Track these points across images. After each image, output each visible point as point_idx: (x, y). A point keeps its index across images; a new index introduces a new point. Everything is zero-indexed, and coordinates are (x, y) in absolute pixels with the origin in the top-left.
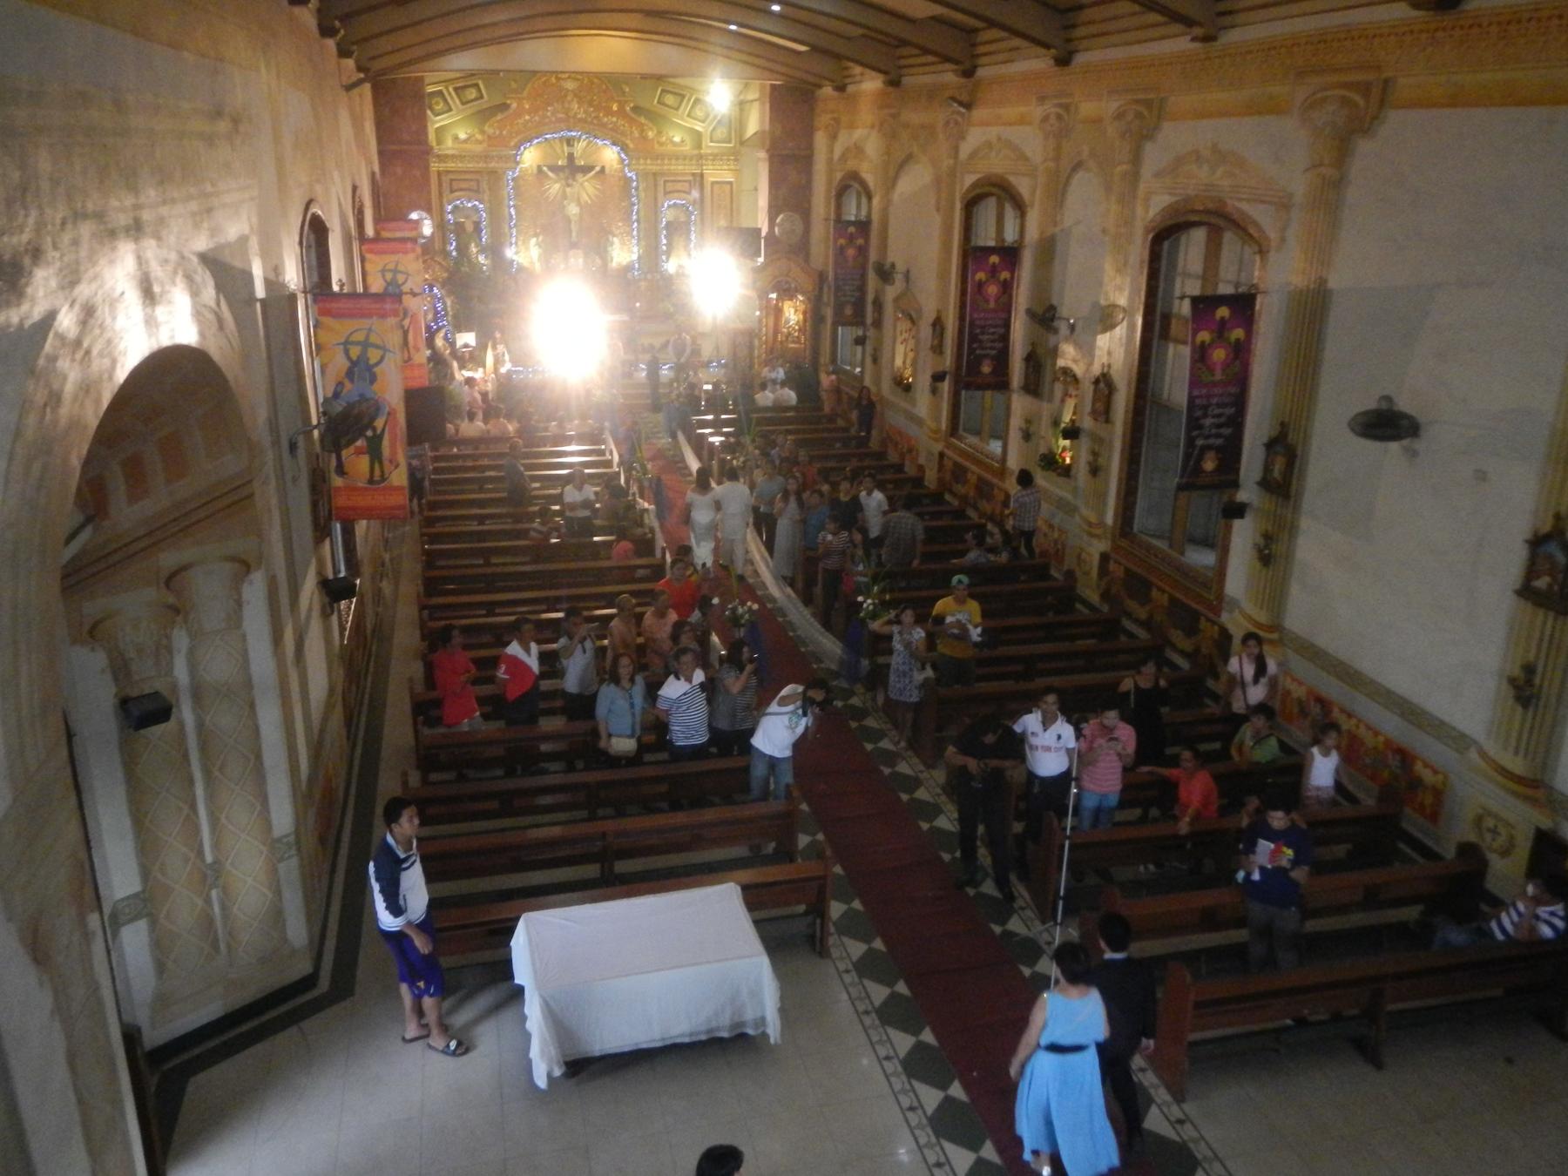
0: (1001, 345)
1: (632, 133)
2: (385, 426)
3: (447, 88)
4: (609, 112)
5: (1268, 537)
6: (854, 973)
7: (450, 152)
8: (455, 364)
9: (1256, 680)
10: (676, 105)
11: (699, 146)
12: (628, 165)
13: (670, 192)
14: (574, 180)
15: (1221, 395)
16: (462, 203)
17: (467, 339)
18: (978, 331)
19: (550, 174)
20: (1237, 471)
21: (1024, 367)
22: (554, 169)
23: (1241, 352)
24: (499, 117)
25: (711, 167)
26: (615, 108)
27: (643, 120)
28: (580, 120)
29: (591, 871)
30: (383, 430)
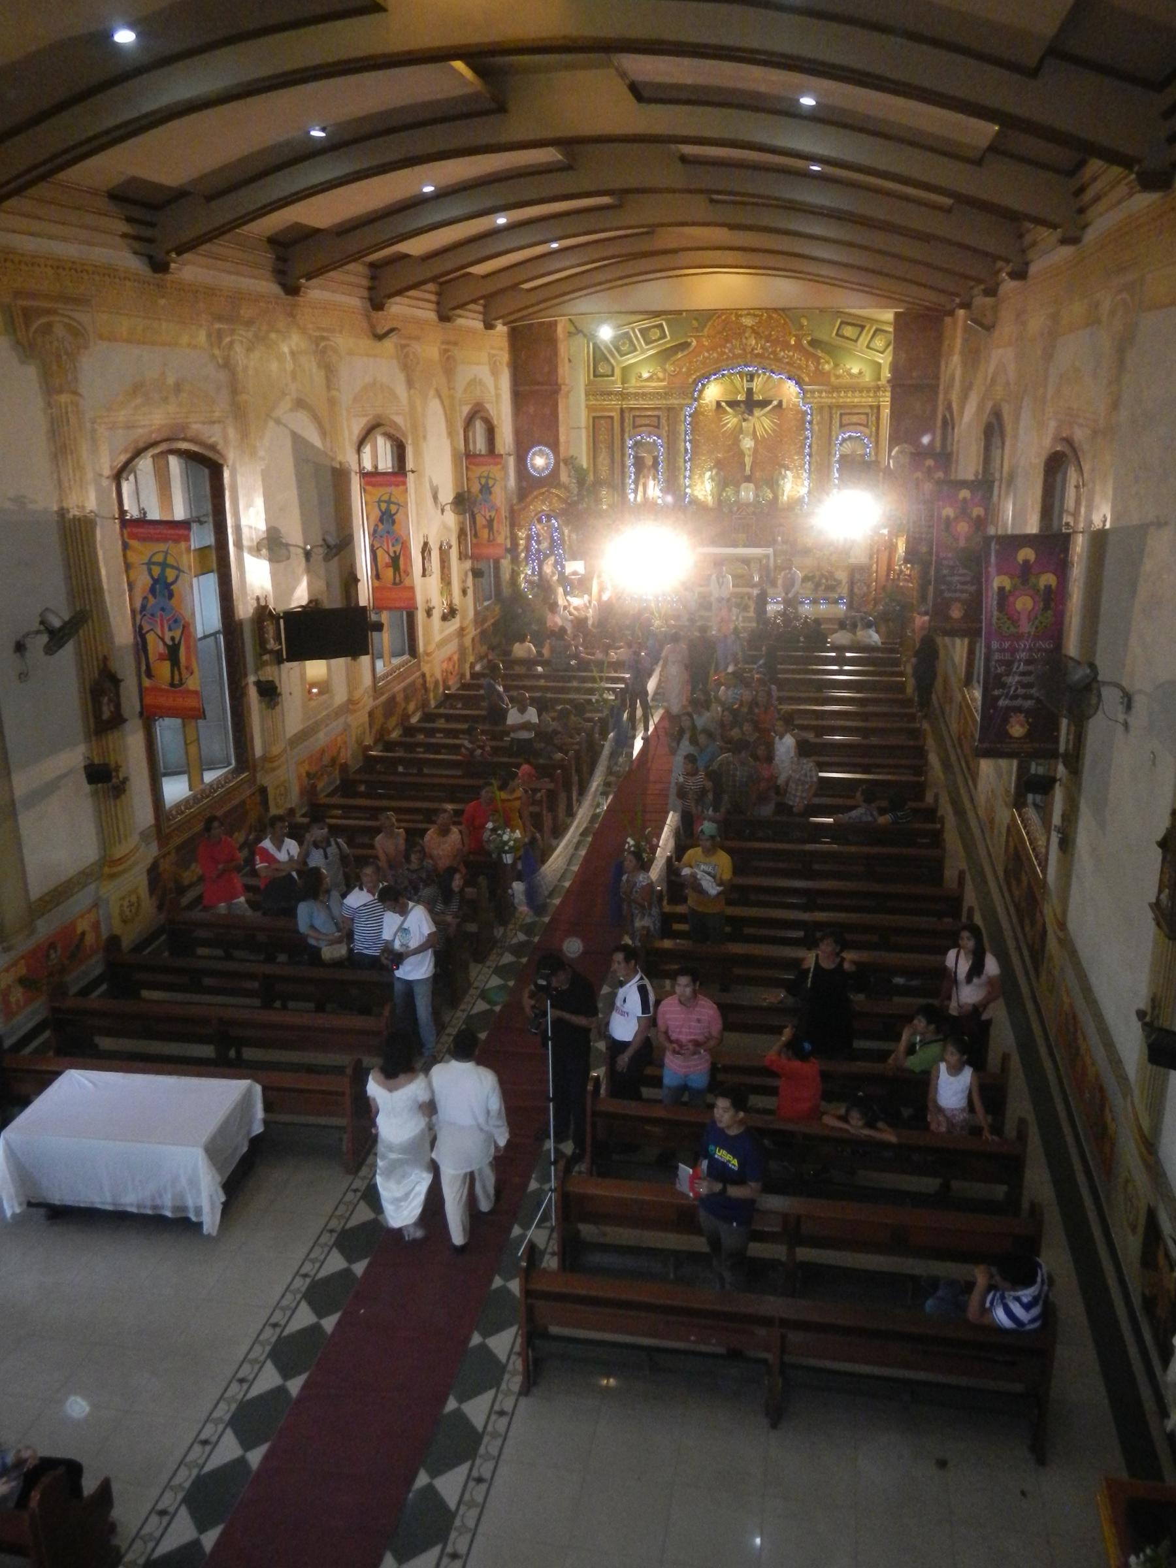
1: (807, 366)
3: (633, 329)
4: (786, 346)
7: (632, 390)
8: (560, 590)
9: (969, 980)
10: (854, 337)
13: (845, 426)
14: (751, 413)
15: (1030, 649)
16: (642, 438)
17: (574, 567)
18: (945, 572)
19: (728, 409)
22: (732, 404)
23: (1054, 599)
24: (680, 355)
27: (820, 353)
28: (757, 355)
29: (206, 1051)
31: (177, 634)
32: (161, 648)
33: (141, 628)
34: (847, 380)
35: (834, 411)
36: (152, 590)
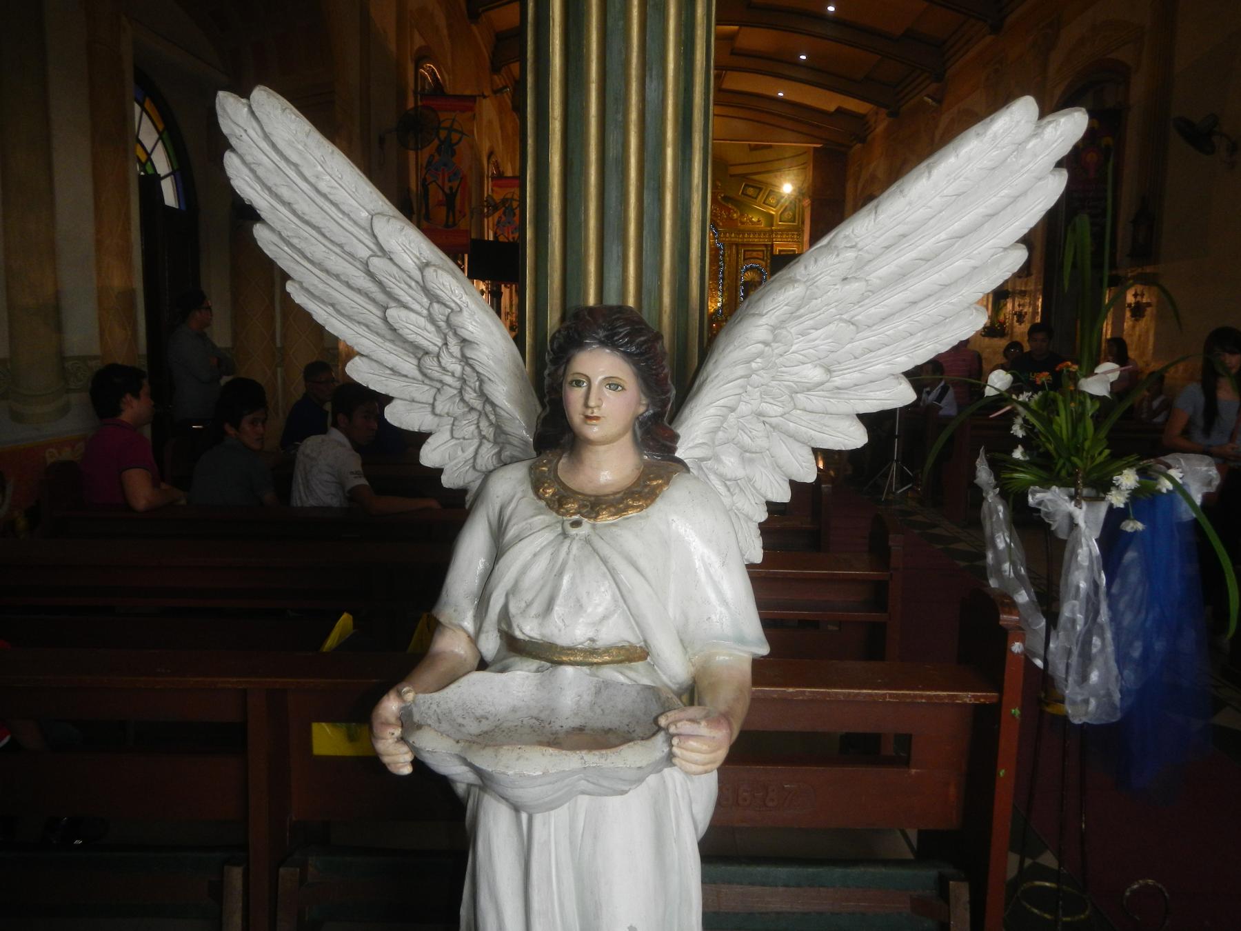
2: (458, 188)
10: (755, 196)
11: (772, 225)
13: (747, 259)
25: (780, 240)
30: (457, 191)
31: (455, 184)
32: (441, 196)
33: (425, 180)
34: (750, 226)
35: (740, 248)
36: (438, 150)
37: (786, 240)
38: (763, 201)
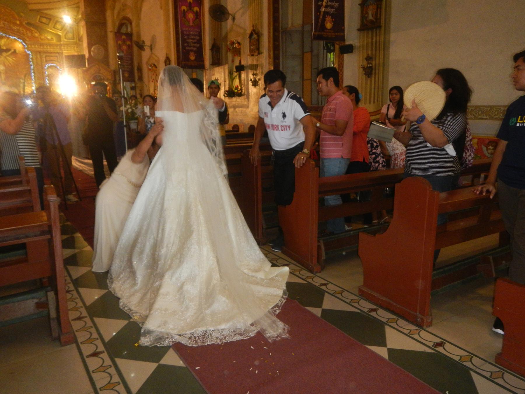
0: (198, 45)
4: (15, 24)
5: (369, 59)
6: (105, 356)
11: (60, 41)
12: (27, 48)
20: (343, 31)
21: (211, 53)
26: (18, 22)
27: (32, 29)
34: (46, 41)
37: (70, 50)
38: (53, 26)
